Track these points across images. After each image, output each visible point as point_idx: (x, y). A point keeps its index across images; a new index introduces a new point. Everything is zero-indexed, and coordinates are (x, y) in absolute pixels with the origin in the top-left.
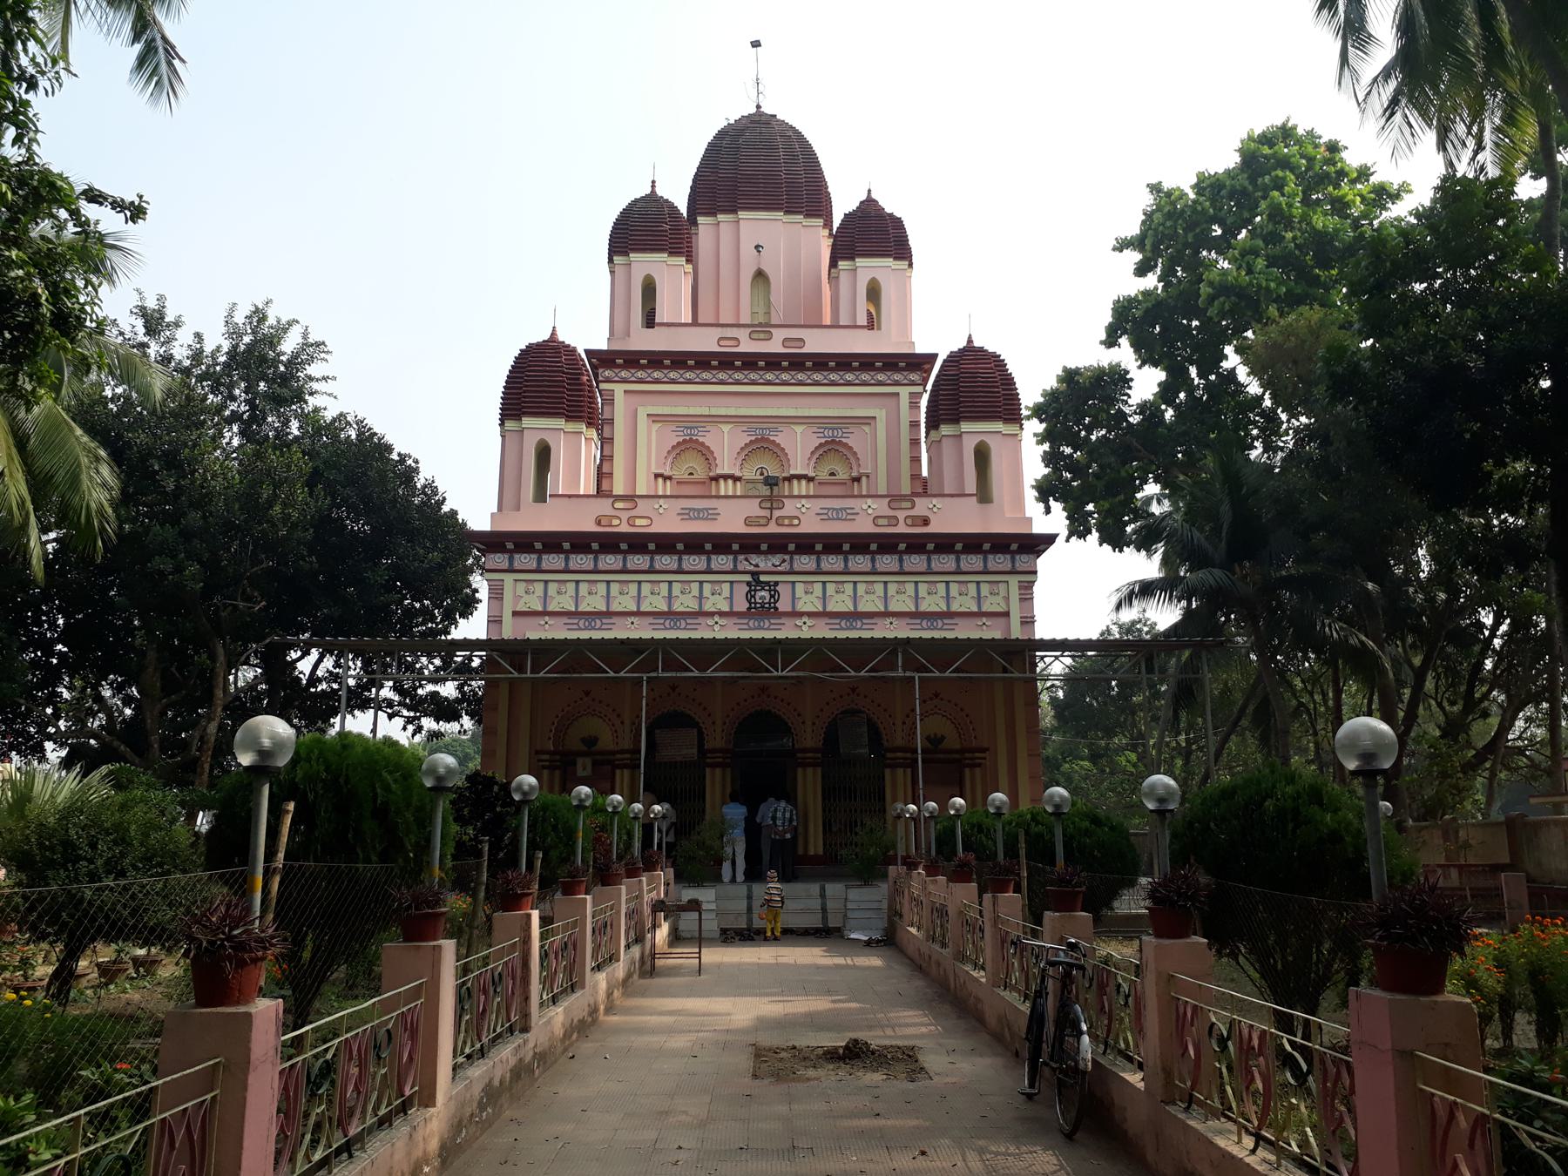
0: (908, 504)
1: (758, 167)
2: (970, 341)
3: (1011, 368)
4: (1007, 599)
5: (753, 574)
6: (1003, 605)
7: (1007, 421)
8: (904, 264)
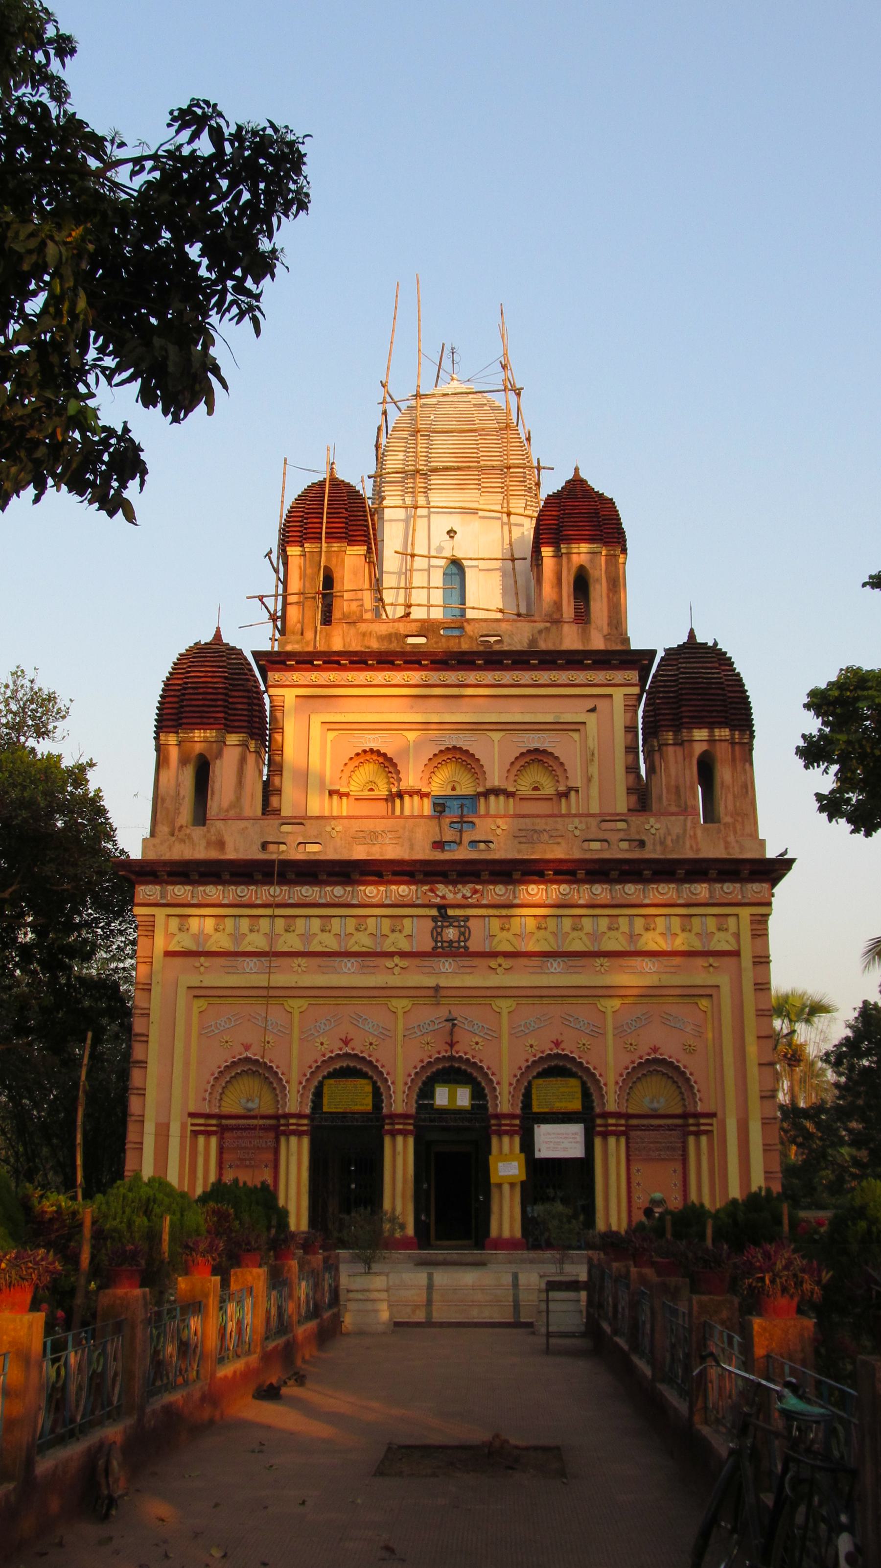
2: (692, 635)
3: (739, 667)
4: (737, 936)
6: (732, 940)
7: (733, 728)
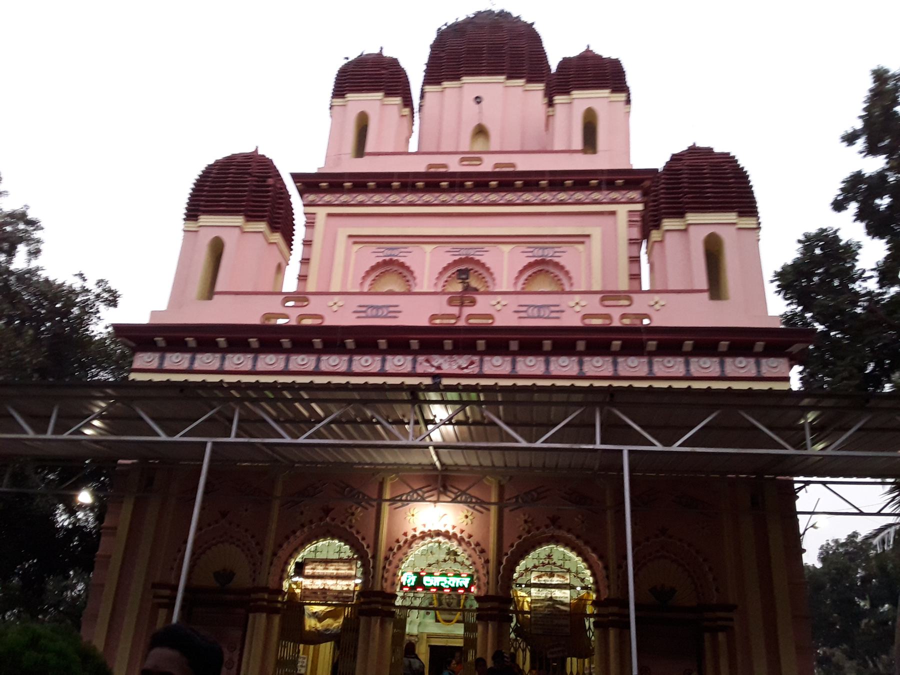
0: (626, 302)
1: (485, 48)
3: (742, 162)
5: (434, 376)
7: (742, 214)
8: (622, 97)
